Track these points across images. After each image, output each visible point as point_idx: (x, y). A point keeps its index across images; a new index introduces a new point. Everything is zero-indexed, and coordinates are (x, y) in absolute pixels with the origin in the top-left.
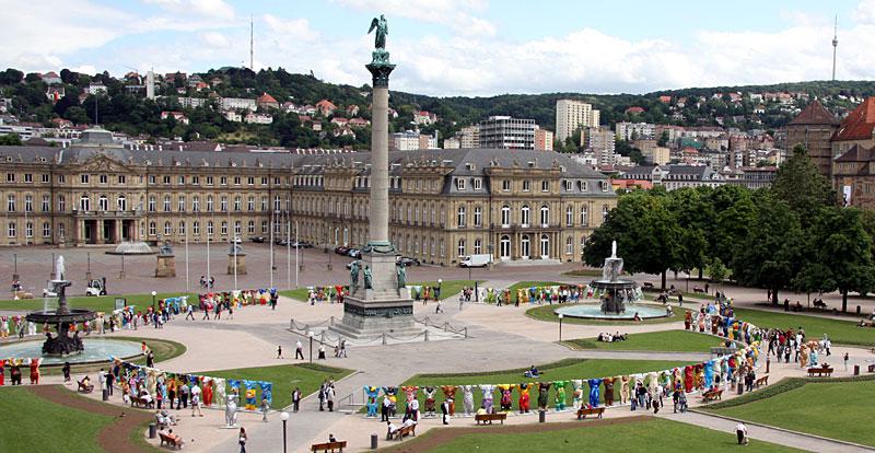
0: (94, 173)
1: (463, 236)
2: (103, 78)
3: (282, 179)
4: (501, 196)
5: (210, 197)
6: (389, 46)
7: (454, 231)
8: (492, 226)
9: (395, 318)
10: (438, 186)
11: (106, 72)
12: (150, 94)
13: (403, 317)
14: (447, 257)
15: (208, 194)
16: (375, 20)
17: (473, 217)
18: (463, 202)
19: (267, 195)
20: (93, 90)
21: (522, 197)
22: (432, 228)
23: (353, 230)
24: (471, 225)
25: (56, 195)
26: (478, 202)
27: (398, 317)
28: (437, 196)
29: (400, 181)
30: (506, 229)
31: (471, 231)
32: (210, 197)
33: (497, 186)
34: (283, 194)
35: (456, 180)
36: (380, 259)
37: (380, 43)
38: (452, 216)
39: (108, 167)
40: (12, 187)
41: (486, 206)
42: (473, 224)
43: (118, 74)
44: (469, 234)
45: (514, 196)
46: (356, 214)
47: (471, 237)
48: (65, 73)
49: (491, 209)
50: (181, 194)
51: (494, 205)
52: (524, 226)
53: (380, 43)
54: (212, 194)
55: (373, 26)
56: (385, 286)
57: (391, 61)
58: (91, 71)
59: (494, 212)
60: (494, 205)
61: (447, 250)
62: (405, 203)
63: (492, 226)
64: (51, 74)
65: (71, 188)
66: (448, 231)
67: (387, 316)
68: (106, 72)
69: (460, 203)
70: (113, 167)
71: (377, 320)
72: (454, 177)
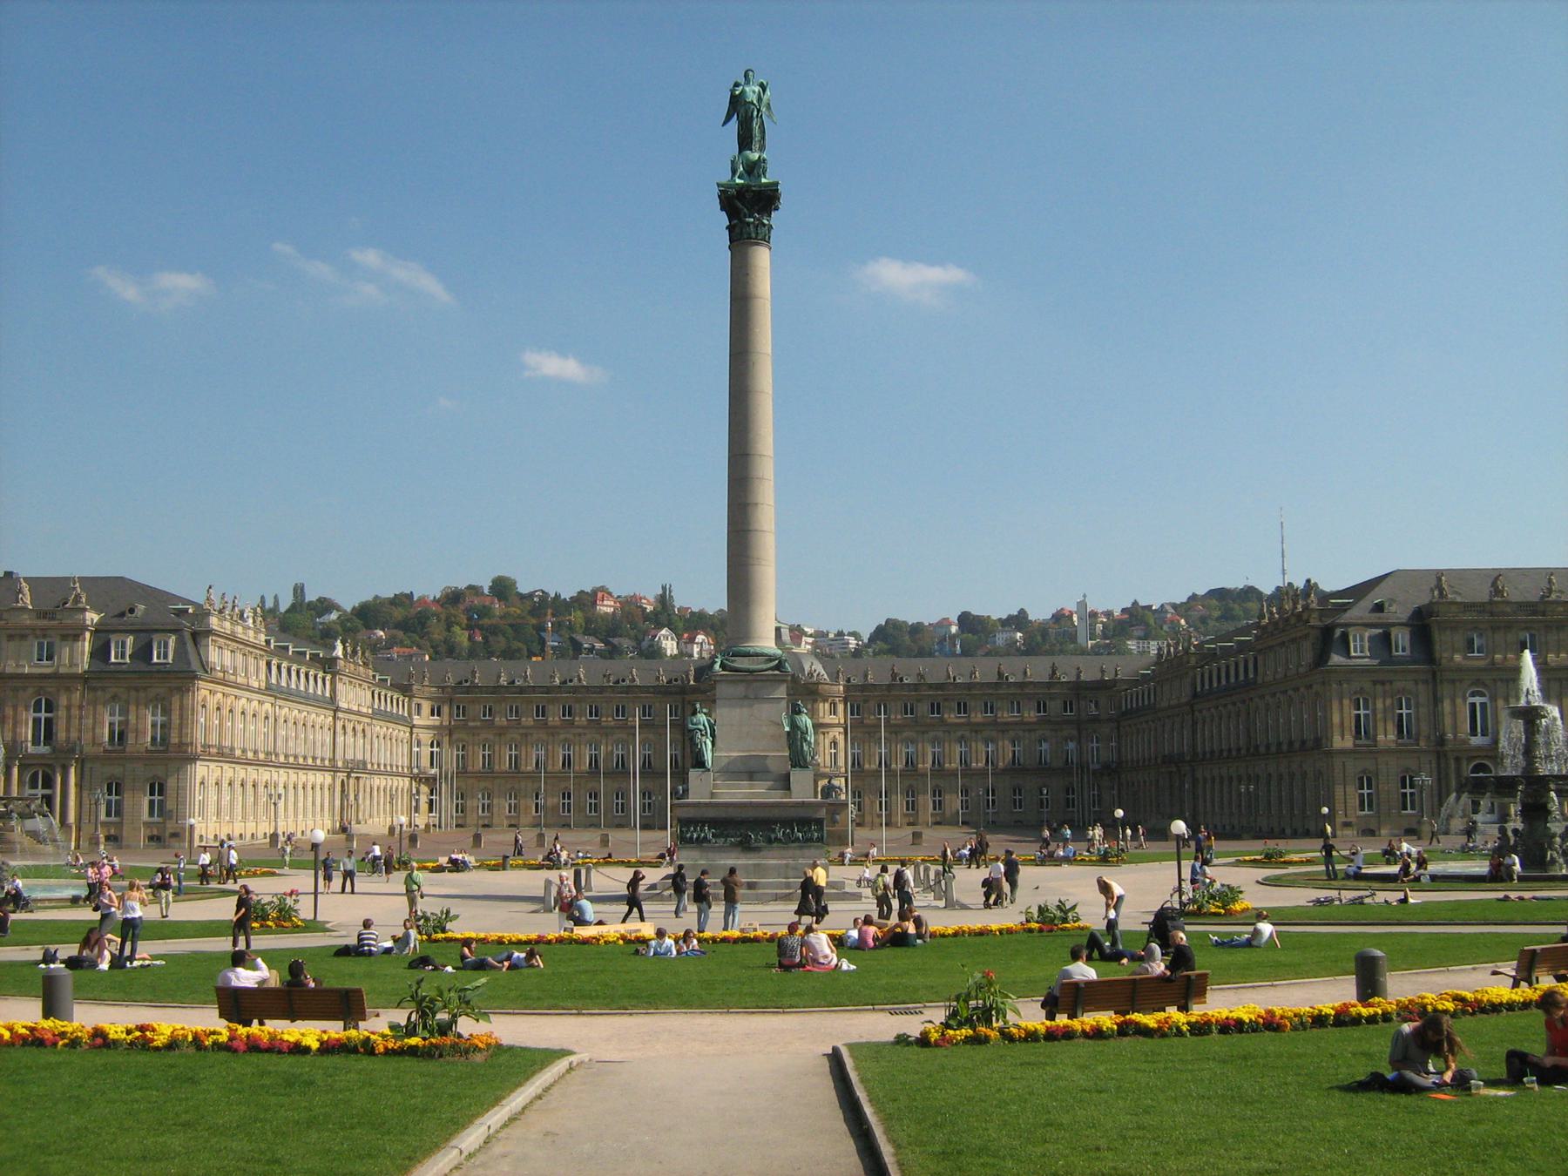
1: (1368, 764)
2: (1018, 620)
7: (1343, 752)
10: (1308, 654)
11: (1022, 612)
15: (959, 734)
19: (1075, 732)
20: (1001, 639)
23: (1195, 782)
35: (1345, 636)
42: (1392, 737)
43: (1039, 613)
48: (966, 620)
54: (967, 734)
68: (1022, 612)
72: (1338, 632)
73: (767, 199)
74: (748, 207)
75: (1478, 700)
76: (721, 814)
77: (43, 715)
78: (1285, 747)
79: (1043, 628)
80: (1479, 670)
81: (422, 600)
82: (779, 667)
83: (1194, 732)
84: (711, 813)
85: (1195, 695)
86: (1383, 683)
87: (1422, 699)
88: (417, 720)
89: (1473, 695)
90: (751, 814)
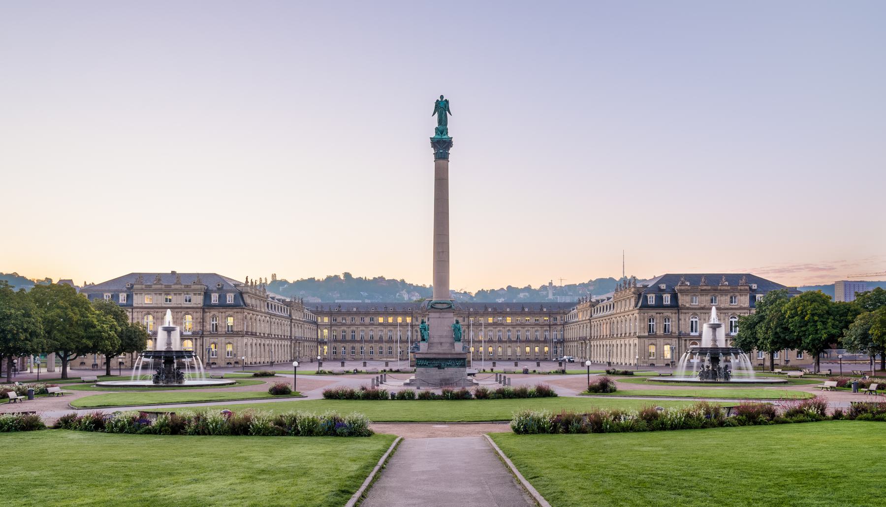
2: (528, 289)
3: (558, 318)
4: (688, 308)
5: (509, 330)
17: (662, 326)
20: (521, 295)
24: (660, 332)
26: (667, 313)
30: (694, 336)
31: (660, 337)
34: (559, 328)
36: (437, 315)
37: (443, 121)
41: (674, 317)
42: (662, 332)
44: (658, 340)
49: (679, 320)
50: (490, 328)
56: (443, 340)
57: (450, 135)
59: (682, 322)
60: (682, 317)
63: (680, 333)
67: (439, 367)
69: (650, 314)
74: (442, 145)
75: (694, 320)
80: (695, 309)
81: (319, 280)
82: (451, 307)
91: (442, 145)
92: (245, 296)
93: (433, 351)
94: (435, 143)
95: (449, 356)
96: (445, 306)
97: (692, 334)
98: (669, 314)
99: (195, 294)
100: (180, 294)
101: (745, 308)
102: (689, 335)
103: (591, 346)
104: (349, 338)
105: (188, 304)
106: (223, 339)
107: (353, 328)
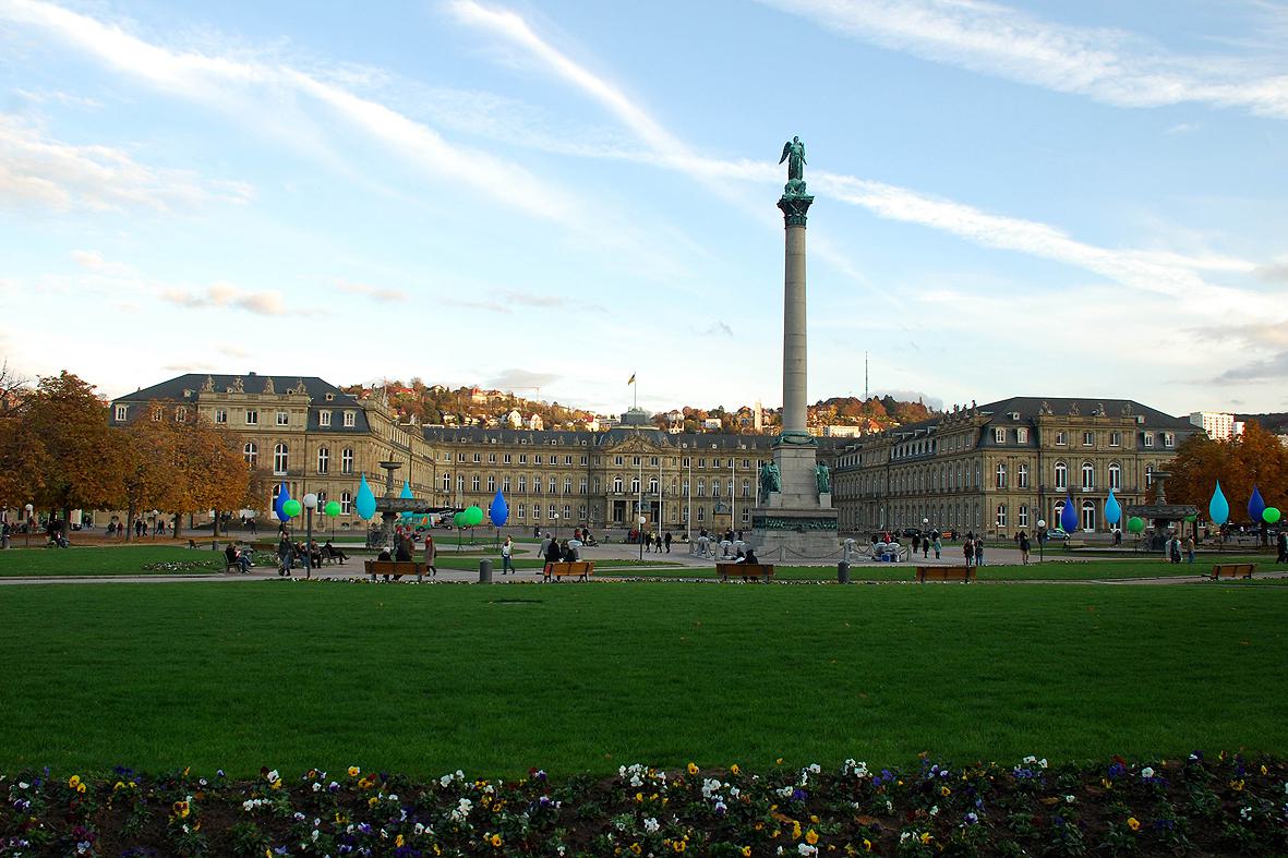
0: (626, 452)
1: (1003, 500)
2: (718, 413)
4: (1052, 451)
6: (808, 176)
7: (991, 493)
8: (1042, 489)
9: (810, 533)
10: (972, 440)
12: (758, 425)
13: (823, 533)
14: (983, 527)
15: (744, 478)
16: (788, 144)
18: (1003, 456)
21: (1082, 452)
22: (967, 492)
23: (889, 508)
24: (1013, 486)
25: (592, 477)
27: (814, 533)
28: (970, 452)
29: (934, 442)
31: (1014, 493)
32: (746, 481)
33: (1046, 437)
35: (994, 431)
36: (793, 453)
37: (795, 172)
38: (988, 476)
39: (641, 446)
40: (569, 469)
43: (731, 408)
45: (1070, 451)
46: (891, 490)
47: (1015, 502)
51: (1045, 463)
52: (1085, 490)
53: (795, 172)
54: (749, 478)
55: (785, 154)
57: (808, 192)
58: (706, 407)
61: (983, 514)
62: (938, 467)
63: (1042, 489)
64: (676, 412)
65: (605, 470)
66: (983, 494)
67: (799, 530)
69: (999, 459)
70: (647, 448)
71: (782, 533)
73: (806, 203)
74: (795, 207)
76: (787, 514)
77: (282, 454)
78: (917, 493)
79: (733, 417)
80: (1062, 451)
83: (889, 481)
84: (782, 514)
85: (890, 460)
86: (1013, 457)
87: (1032, 467)
88: (437, 462)
89: (1058, 465)
90: (802, 514)
91: (795, 207)
92: (370, 415)
93: (788, 506)
94: (783, 204)
95: (814, 515)
96: (803, 440)
97: (1085, 490)
98: (1027, 460)
99: (294, 411)
100: (270, 410)
101: (1130, 452)
102: (1054, 490)
103: (889, 508)
104: (485, 488)
105: (283, 427)
106: (337, 483)
107: (492, 472)
